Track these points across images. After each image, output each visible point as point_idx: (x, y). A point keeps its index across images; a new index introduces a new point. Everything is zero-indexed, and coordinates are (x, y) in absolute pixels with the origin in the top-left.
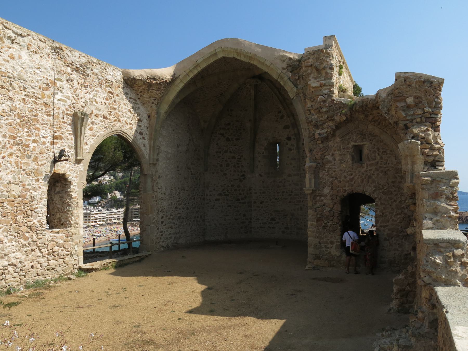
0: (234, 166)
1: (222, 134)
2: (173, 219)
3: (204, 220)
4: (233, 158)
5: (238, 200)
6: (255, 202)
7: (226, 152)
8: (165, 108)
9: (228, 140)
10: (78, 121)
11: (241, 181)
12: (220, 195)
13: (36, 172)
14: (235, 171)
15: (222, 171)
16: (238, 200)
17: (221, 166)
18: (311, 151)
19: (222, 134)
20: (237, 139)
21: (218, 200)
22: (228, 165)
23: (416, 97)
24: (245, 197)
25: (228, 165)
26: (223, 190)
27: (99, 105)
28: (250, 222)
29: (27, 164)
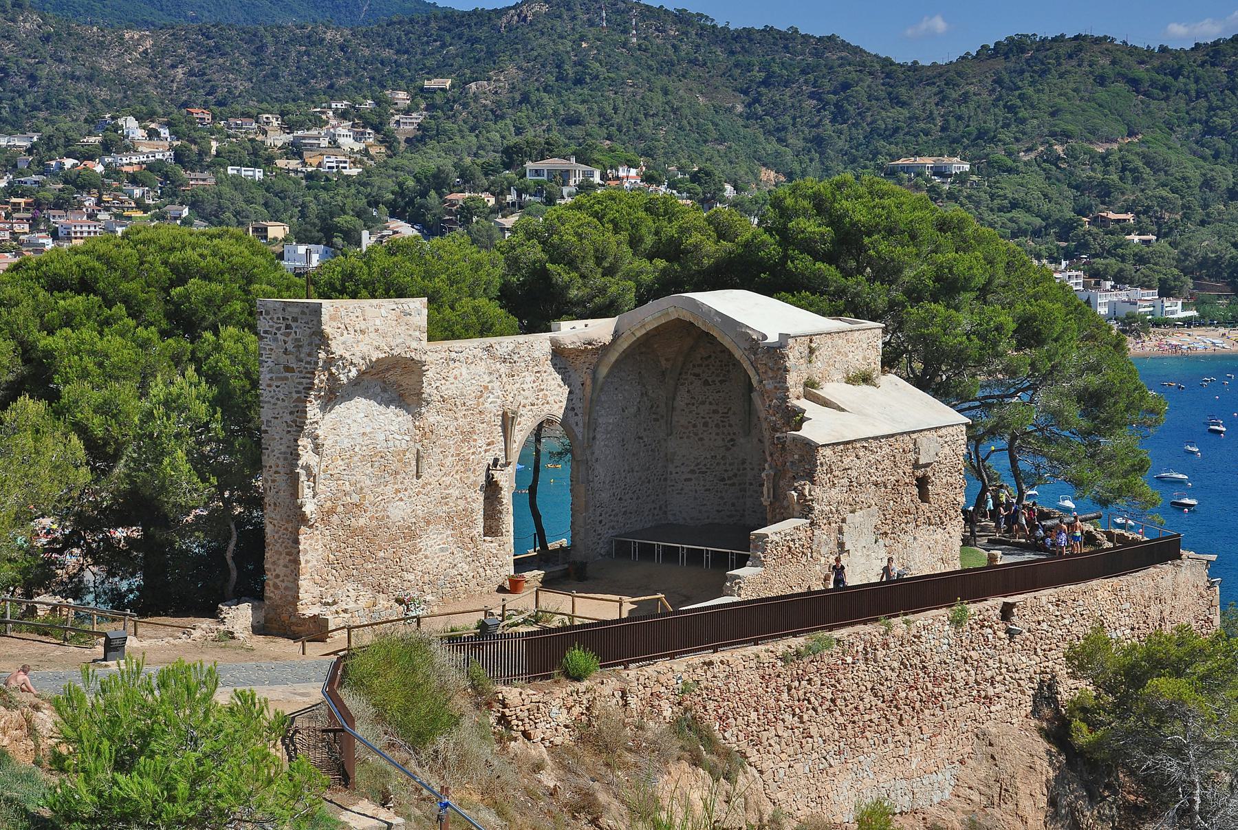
0: (717, 426)
1: (697, 375)
2: (616, 515)
3: (665, 513)
4: (715, 412)
5: (723, 480)
6: (751, 484)
7: (703, 403)
8: (604, 371)
9: (706, 383)
10: (507, 422)
11: (728, 449)
12: (693, 472)
13: (475, 483)
14: (717, 434)
15: (696, 434)
16: (723, 480)
17: (695, 426)
18: (771, 455)
19: (697, 375)
20: (721, 382)
21: (690, 480)
22: (706, 424)
23: (801, 456)
24: (735, 475)
25: (706, 424)
26: (698, 464)
27: (526, 393)
28: (743, 516)
29: (468, 478)
